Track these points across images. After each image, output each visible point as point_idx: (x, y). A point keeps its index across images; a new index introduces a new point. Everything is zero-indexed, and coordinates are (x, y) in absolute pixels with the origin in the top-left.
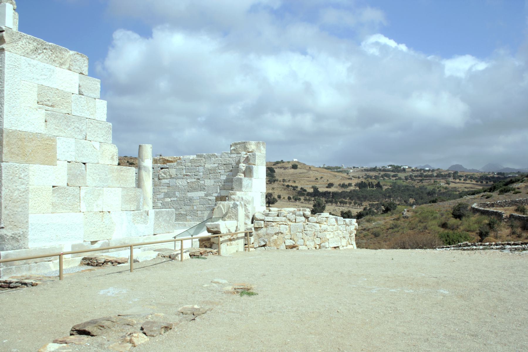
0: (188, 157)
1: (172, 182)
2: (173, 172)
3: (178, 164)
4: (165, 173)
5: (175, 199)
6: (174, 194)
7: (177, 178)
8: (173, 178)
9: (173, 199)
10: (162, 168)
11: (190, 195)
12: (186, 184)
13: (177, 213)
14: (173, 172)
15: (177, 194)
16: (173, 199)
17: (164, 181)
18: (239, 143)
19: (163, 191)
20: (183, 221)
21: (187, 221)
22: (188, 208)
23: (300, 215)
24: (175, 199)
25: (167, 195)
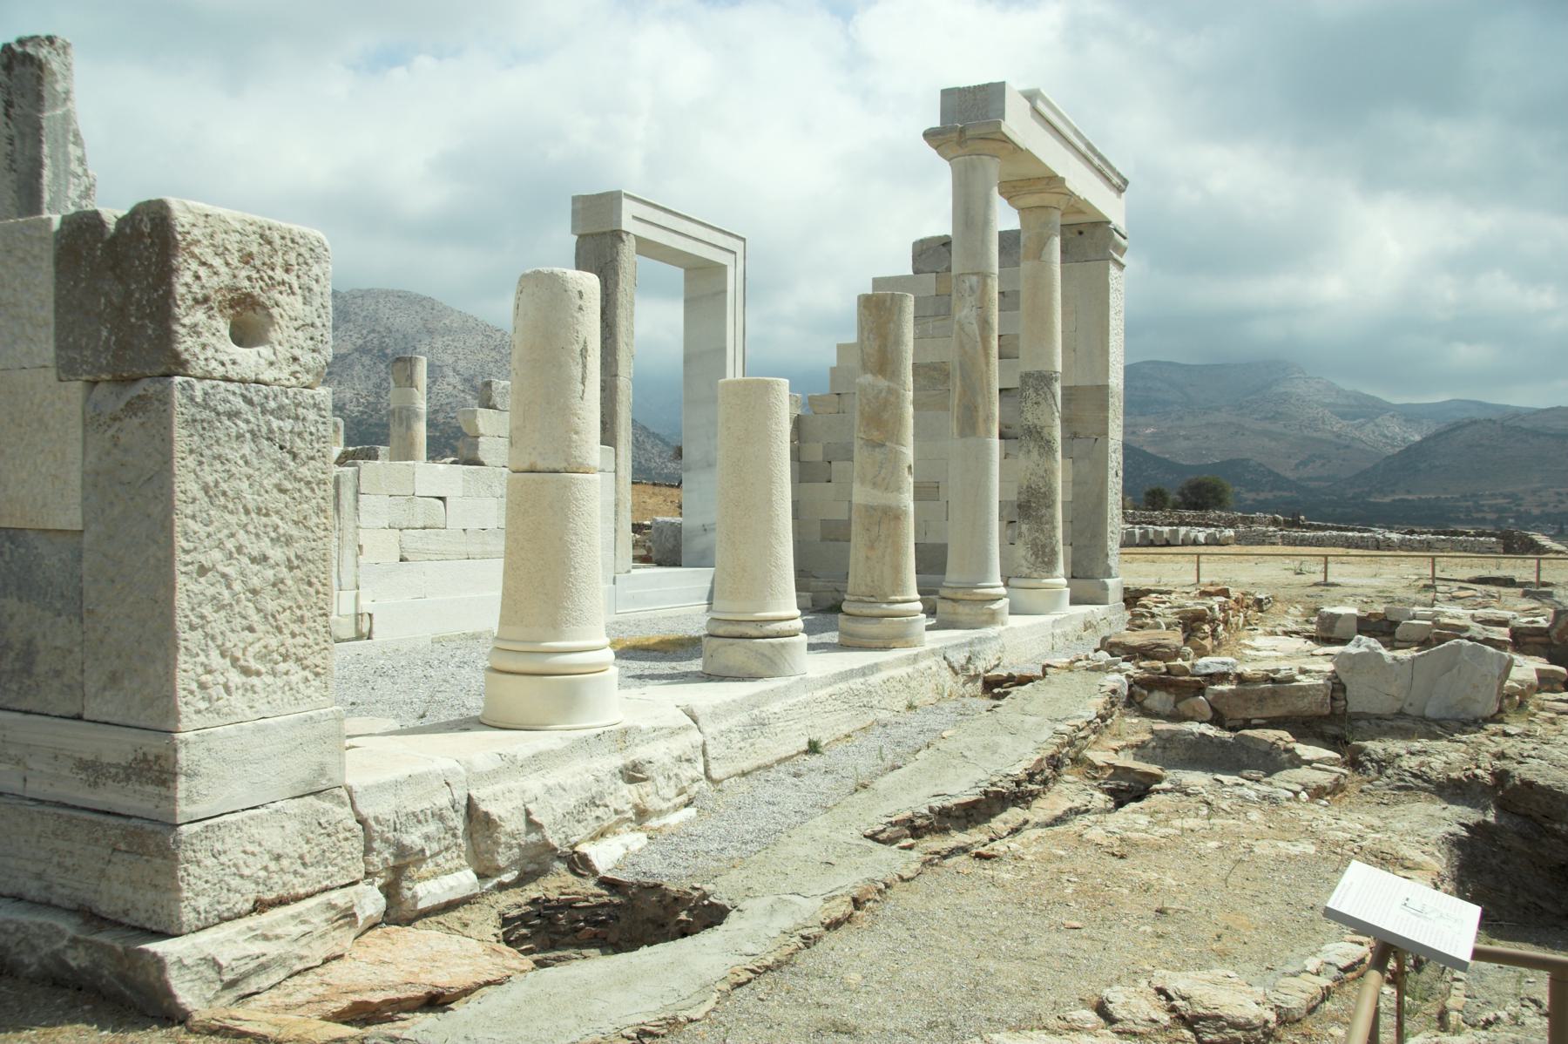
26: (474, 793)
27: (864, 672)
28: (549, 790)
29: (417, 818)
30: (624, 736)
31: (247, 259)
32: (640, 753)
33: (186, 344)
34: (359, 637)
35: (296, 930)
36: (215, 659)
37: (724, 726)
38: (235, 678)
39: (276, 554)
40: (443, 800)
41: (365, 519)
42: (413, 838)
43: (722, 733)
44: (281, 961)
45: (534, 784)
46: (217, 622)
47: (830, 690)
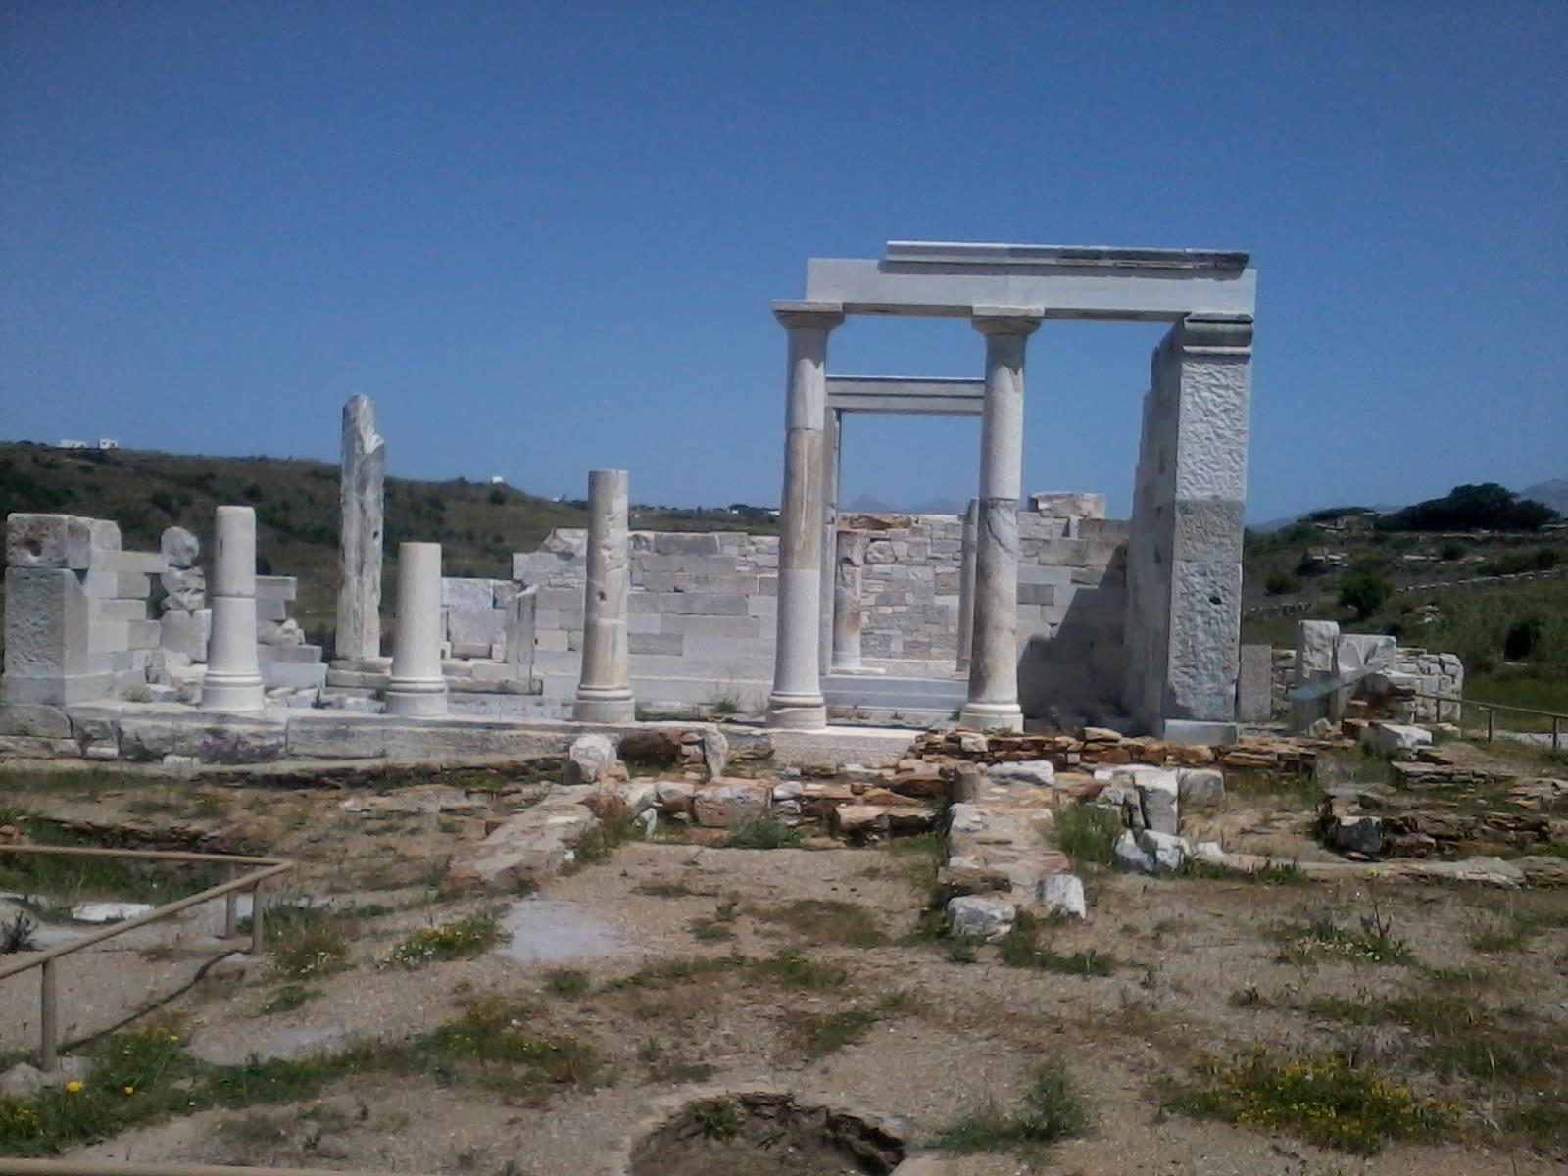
0: (939, 517)
1: (898, 571)
2: (901, 549)
3: (916, 532)
4: (881, 552)
5: (904, 608)
6: (902, 597)
7: (910, 563)
8: (901, 563)
9: (898, 608)
10: (873, 540)
11: (939, 600)
12: (931, 577)
13: (909, 638)
14: (901, 549)
15: (909, 598)
16: (898, 608)
17: (877, 568)
18: (1058, 497)
19: (876, 589)
20: (924, 657)
21: (930, 657)
22: (935, 629)
23: (1434, 662)
24: (904, 608)
25: (884, 599)
26: (122, 721)
27: (489, 726)
28: (154, 727)
29: (92, 723)
30: (223, 717)
31: (32, 529)
32: (226, 727)
33: (10, 558)
34: (533, 693)
35: (24, 743)
36: (19, 654)
37: (307, 728)
38: (26, 661)
39: (42, 622)
40: (106, 719)
41: (537, 621)
42: (88, 729)
43: (302, 732)
44: (11, 750)
45: (148, 723)
46: (18, 641)
47: (435, 730)
